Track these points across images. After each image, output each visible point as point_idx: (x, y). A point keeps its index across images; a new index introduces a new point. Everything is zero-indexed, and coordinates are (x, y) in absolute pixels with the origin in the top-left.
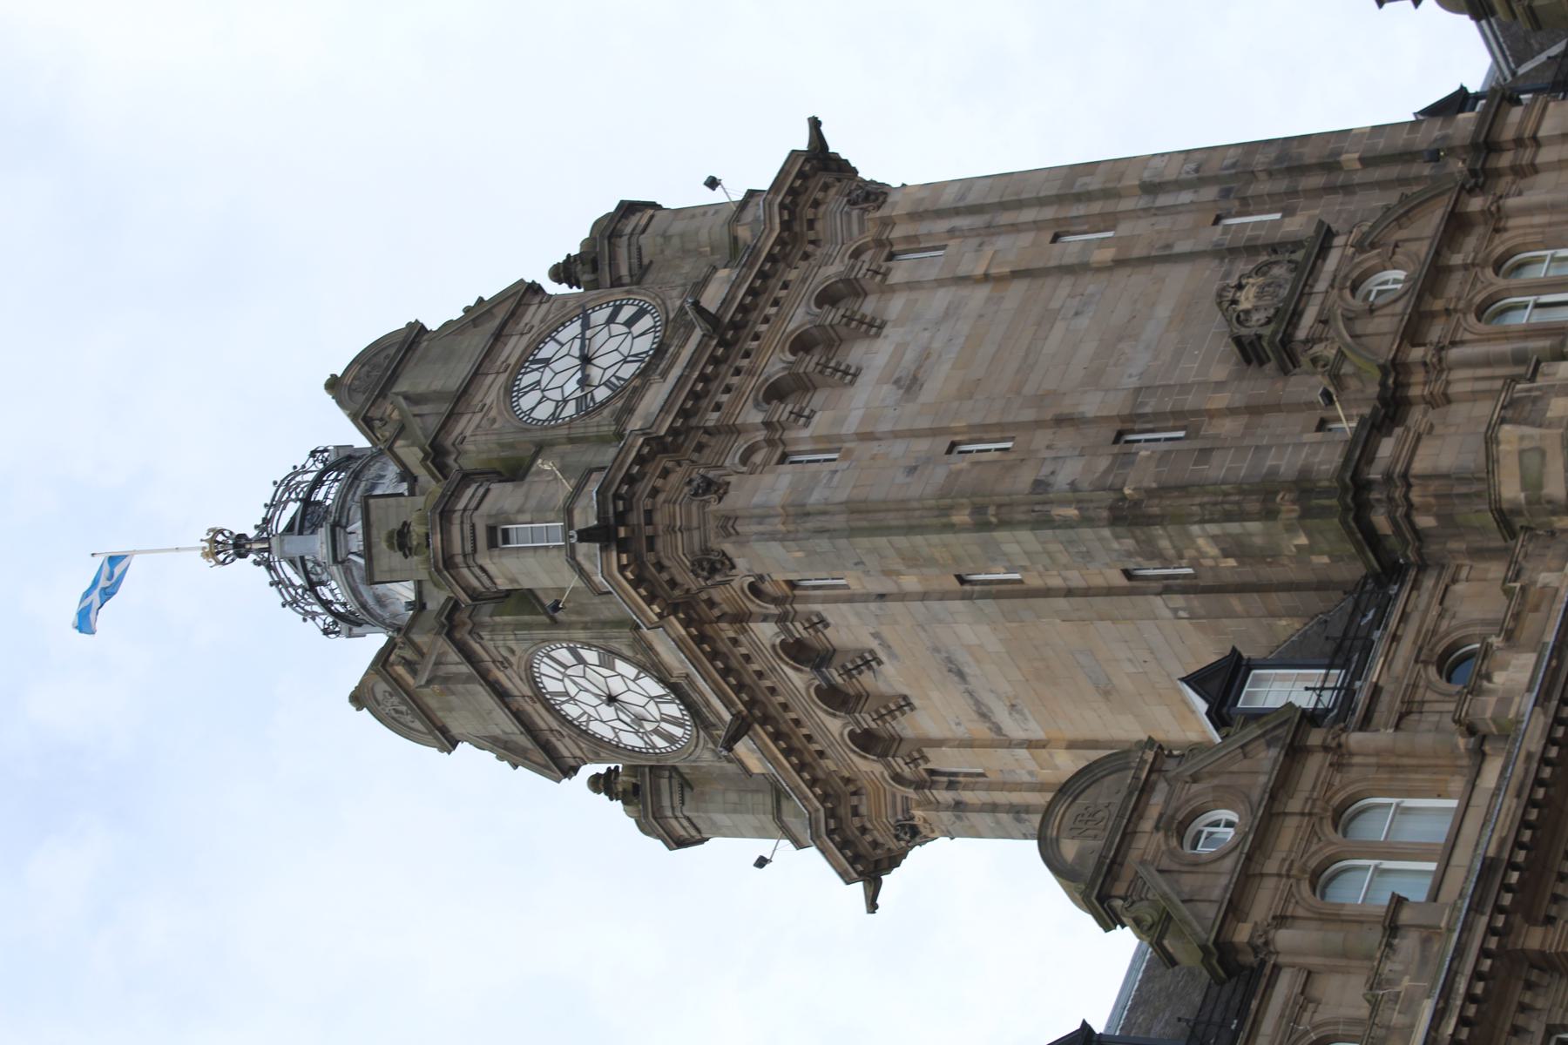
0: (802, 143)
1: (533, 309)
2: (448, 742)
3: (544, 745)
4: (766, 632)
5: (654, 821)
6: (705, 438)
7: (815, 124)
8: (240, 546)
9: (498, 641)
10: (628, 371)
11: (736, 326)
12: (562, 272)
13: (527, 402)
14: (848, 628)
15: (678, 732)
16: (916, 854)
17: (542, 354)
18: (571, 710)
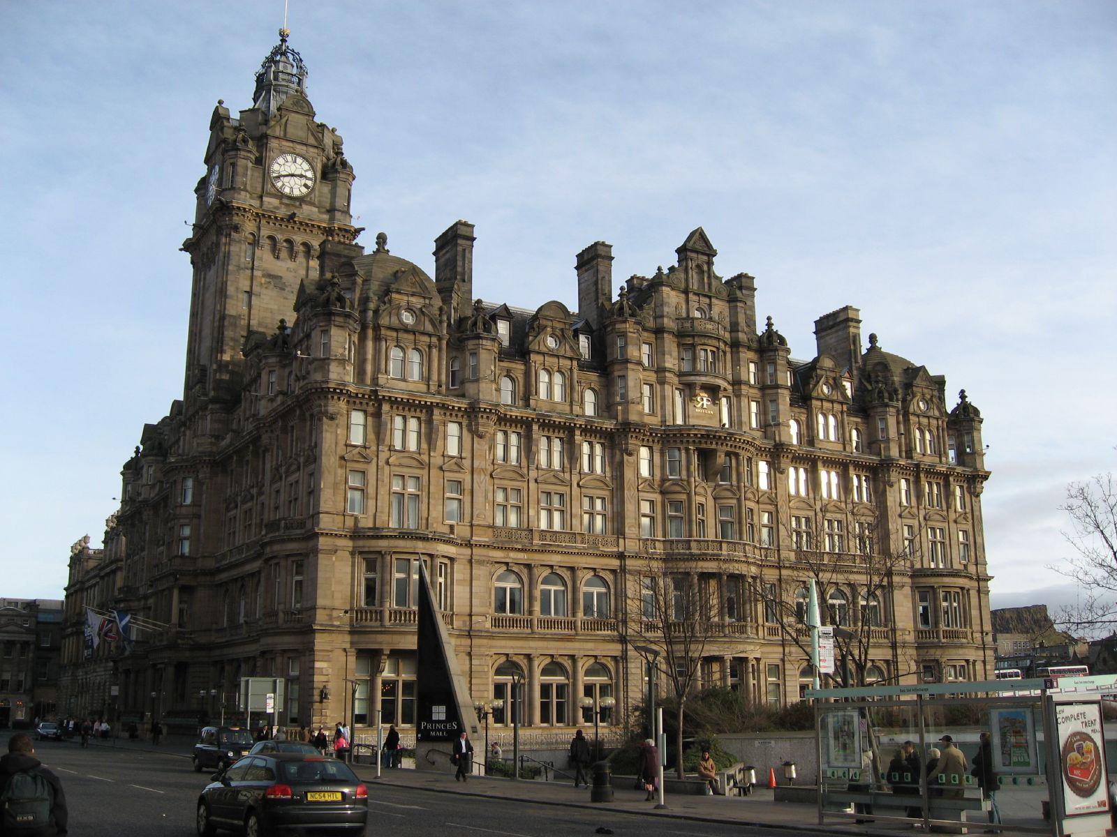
1: (316, 150)
2: (211, 128)
6: (258, 220)
8: (283, 41)
10: (287, 190)
11: (295, 222)
13: (281, 160)
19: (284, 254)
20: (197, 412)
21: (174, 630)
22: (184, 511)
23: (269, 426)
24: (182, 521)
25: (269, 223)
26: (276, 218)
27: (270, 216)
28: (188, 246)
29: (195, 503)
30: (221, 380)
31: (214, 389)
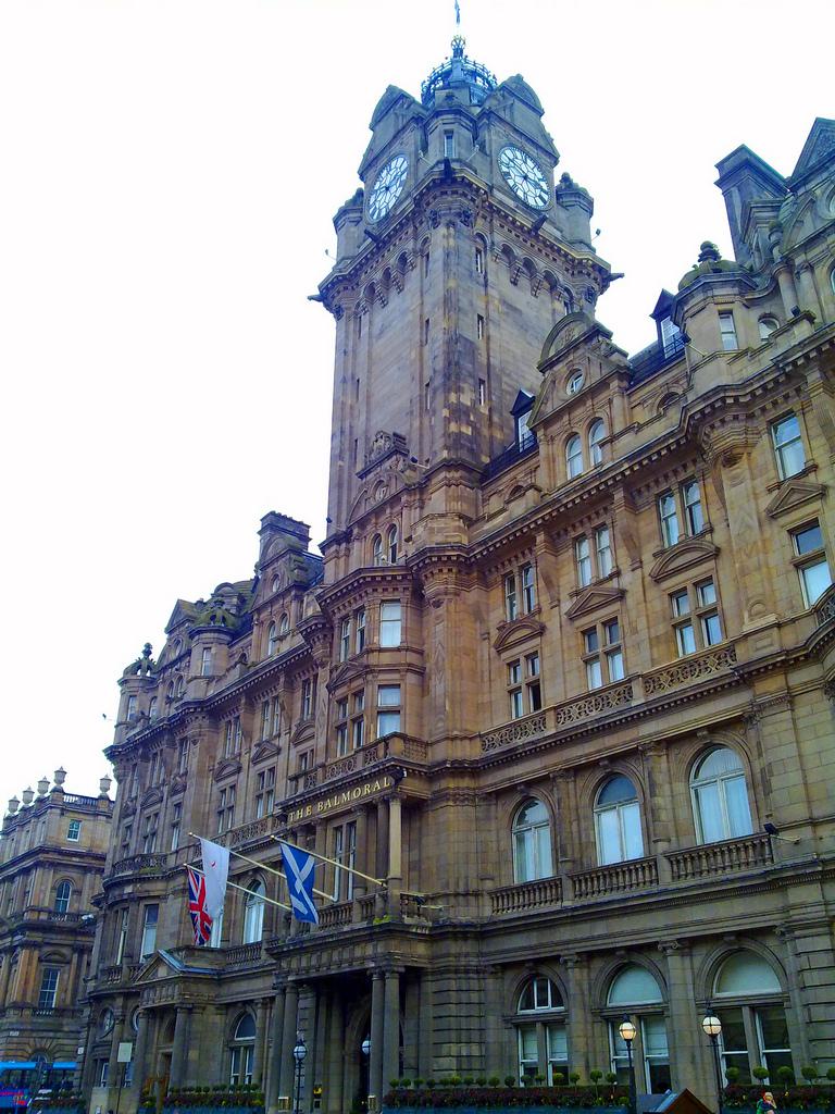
0: (614, 271)
2: (372, 128)
3: (371, 166)
4: (410, 245)
5: (343, 212)
6: (488, 219)
7: (621, 276)
8: (458, 52)
9: (412, 137)
11: (537, 236)
12: (565, 178)
13: (508, 152)
14: (414, 277)
15: (375, 217)
16: (330, 316)
17: (528, 161)
18: (383, 175)
19: (524, 281)
20: (395, 499)
21: (396, 892)
22: (385, 659)
23: (747, 404)
24: (381, 677)
25: (503, 227)
26: (514, 222)
27: (506, 216)
28: (328, 295)
29: (414, 646)
30: (460, 435)
31: (446, 447)
